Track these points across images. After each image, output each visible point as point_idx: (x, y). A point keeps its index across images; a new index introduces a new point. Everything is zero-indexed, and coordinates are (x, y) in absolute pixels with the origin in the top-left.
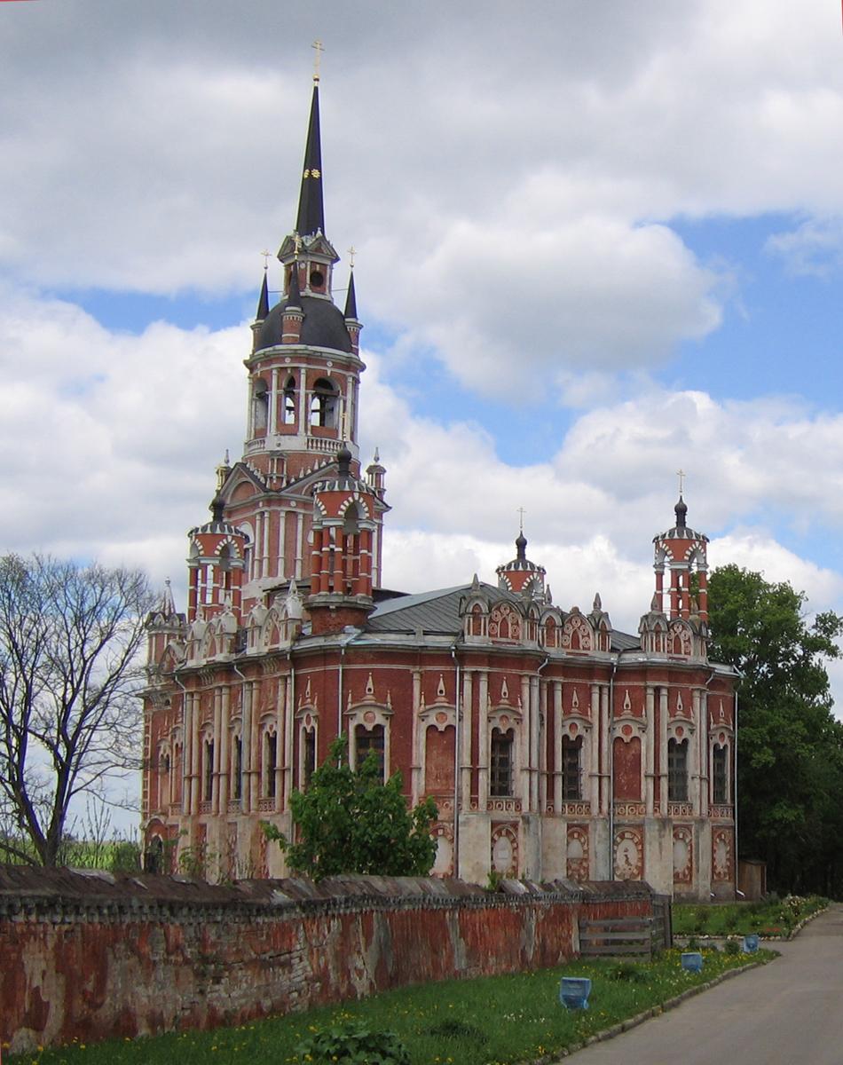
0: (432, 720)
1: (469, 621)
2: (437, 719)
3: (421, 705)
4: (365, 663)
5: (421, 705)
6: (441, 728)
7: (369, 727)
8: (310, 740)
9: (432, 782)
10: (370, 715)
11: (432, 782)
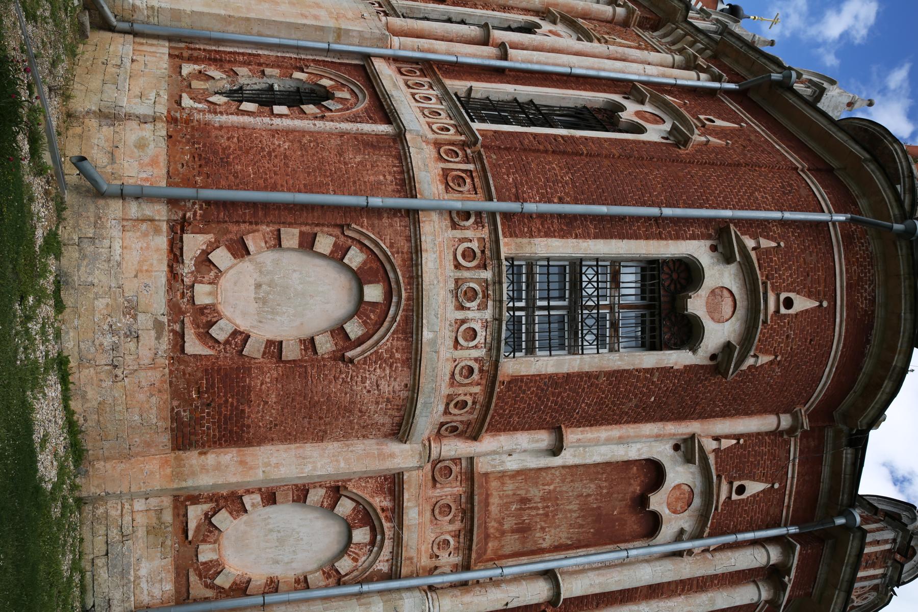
0: (679, 475)
1: (886, 542)
2: (674, 488)
3: (717, 439)
4: (851, 287)
5: (717, 439)
6: (658, 502)
7: (696, 305)
8: (607, 117)
9: (510, 487)
10: (727, 307)
11: (510, 487)
